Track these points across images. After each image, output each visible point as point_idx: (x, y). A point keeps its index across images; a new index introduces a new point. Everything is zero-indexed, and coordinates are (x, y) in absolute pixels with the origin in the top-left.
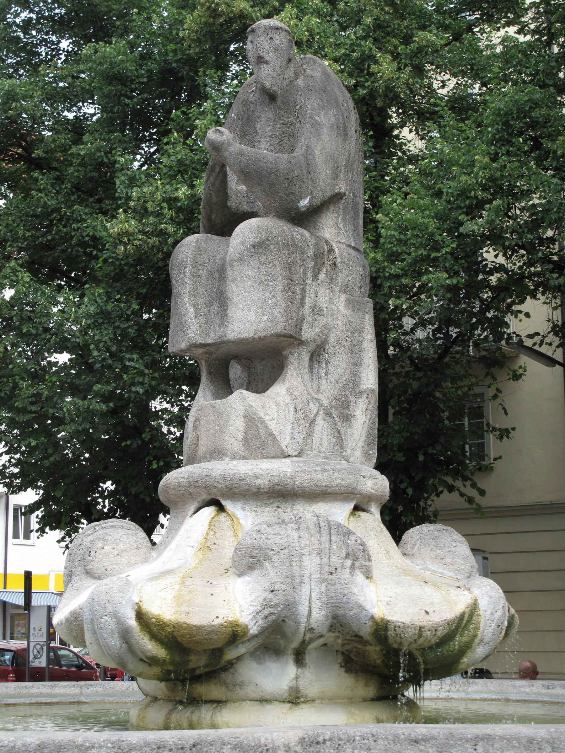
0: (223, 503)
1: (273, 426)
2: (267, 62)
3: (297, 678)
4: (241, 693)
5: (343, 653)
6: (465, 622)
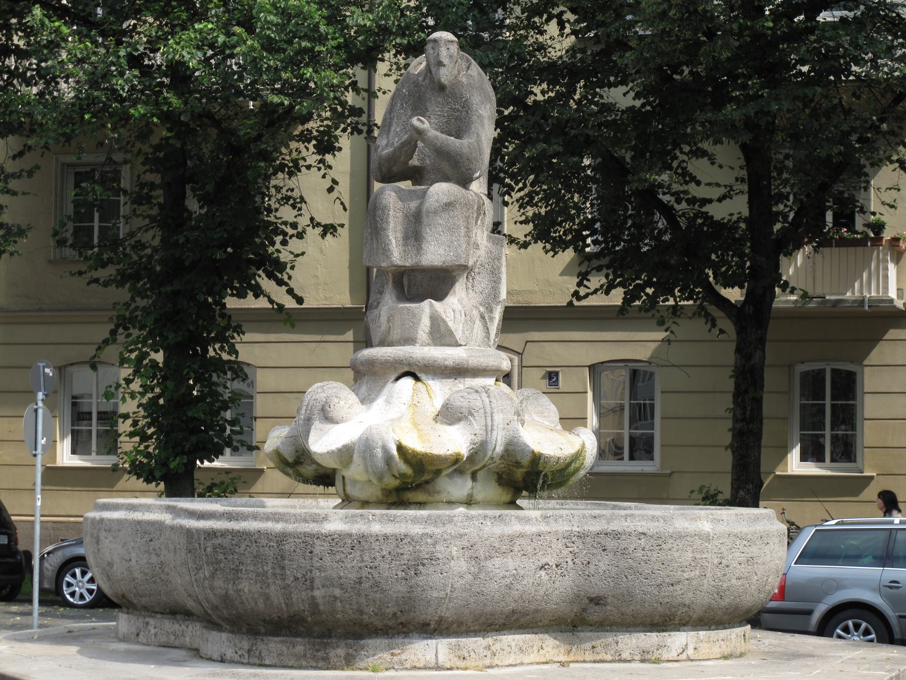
0: (419, 375)
1: (450, 324)
2: (444, 66)
3: (472, 488)
4: (437, 497)
5: (498, 473)
6: (578, 456)
